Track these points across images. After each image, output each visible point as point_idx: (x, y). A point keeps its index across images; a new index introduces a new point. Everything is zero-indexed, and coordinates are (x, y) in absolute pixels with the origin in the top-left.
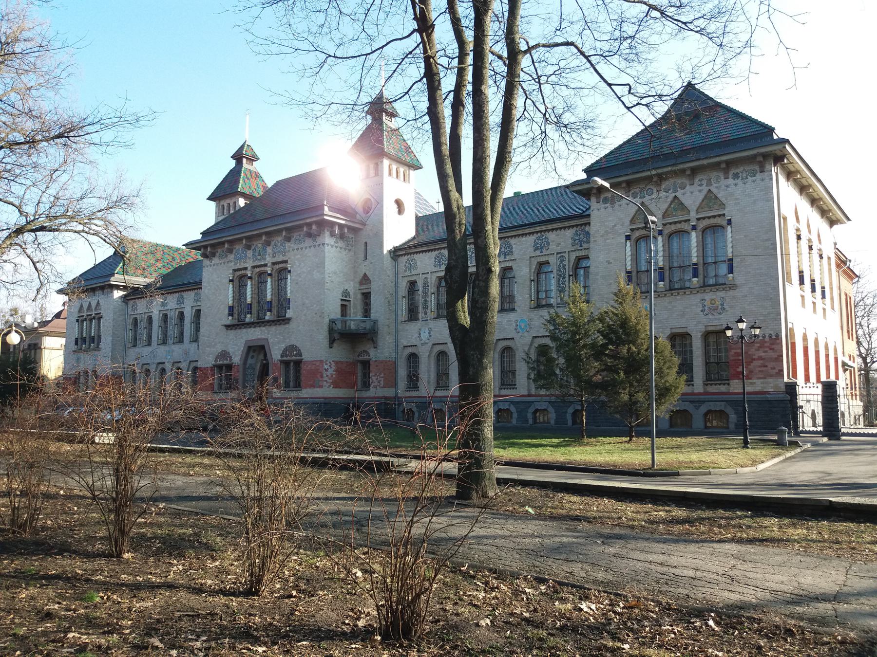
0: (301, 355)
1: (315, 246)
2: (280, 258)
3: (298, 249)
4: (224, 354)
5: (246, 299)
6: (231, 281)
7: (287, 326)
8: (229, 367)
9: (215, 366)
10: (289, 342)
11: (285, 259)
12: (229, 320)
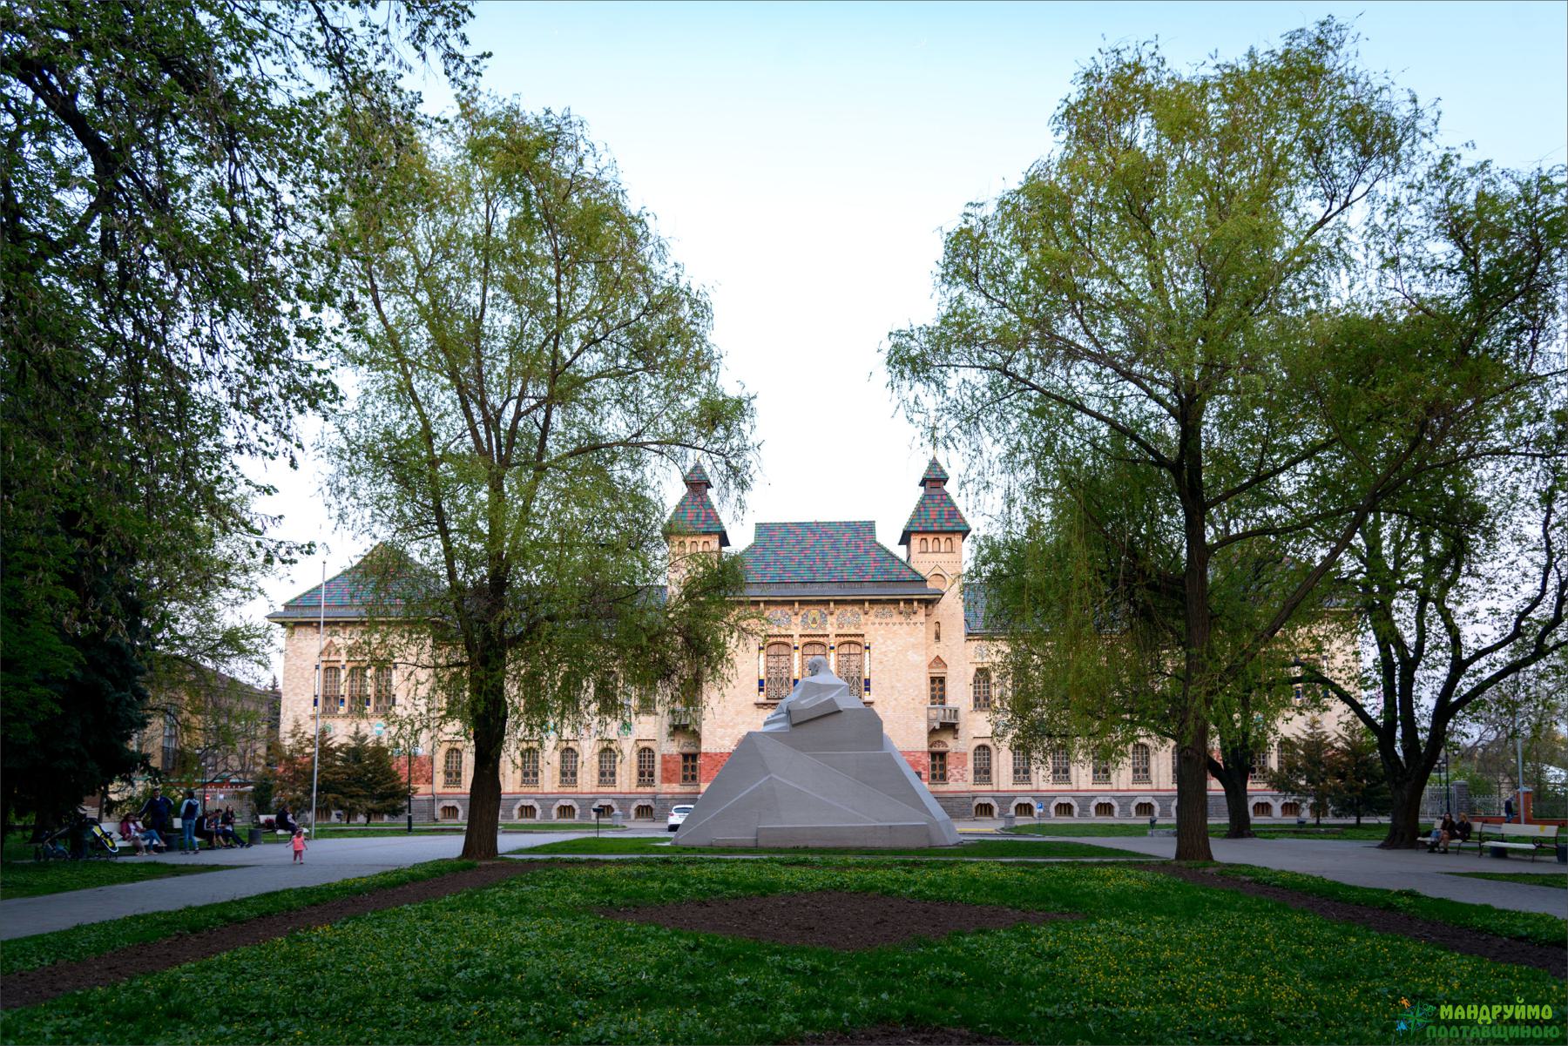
2: (853, 631)
5: (790, 671)
12: (762, 698)
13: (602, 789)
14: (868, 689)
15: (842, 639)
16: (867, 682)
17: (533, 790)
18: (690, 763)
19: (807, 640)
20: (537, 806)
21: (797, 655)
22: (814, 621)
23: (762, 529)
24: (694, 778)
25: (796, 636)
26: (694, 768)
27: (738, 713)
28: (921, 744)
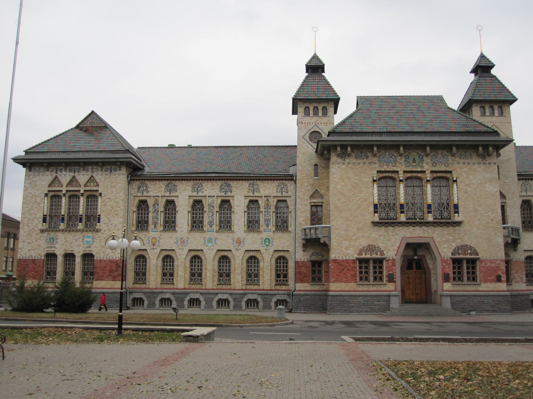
0: (477, 254)
1: (485, 164)
2: (443, 168)
3: (464, 163)
4: (371, 248)
6: (374, 181)
7: (457, 228)
8: (379, 262)
9: (357, 259)
10: (459, 242)
11: (448, 169)
12: (376, 218)
13: (249, 287)
14: (457, 212)
15: (435, 175)
16: (456, 207)
17: (198, 286)
18: (317, 268)
19: (409, 175)
20: (202, 299)
21: (402, 186)
22: (414, 161)
23: (361, 101)
24: (320, 279)
25: (401, 172)
26: (320, 272)
27: (359, 229)
28: (501, 255)
